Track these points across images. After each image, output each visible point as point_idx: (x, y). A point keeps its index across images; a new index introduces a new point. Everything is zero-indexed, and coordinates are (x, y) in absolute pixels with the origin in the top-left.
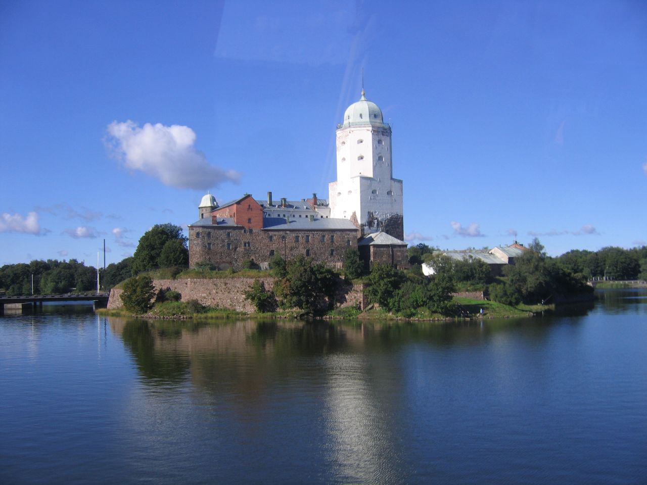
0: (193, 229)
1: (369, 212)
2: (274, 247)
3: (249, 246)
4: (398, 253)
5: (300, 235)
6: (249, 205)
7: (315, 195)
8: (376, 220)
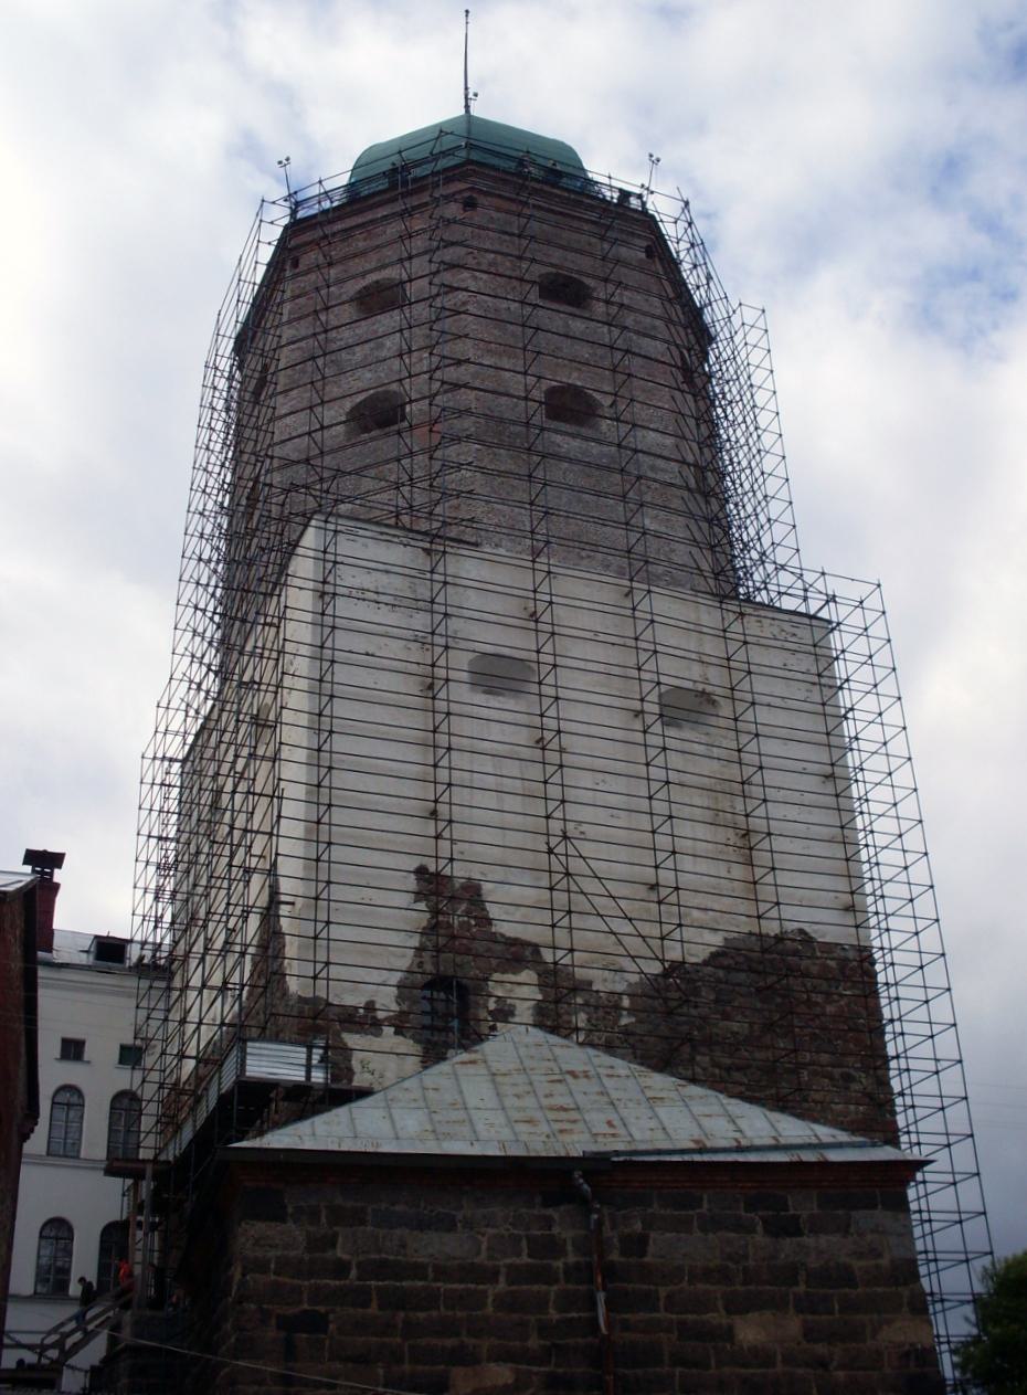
4: (750, 1332)
8: (528, 976)
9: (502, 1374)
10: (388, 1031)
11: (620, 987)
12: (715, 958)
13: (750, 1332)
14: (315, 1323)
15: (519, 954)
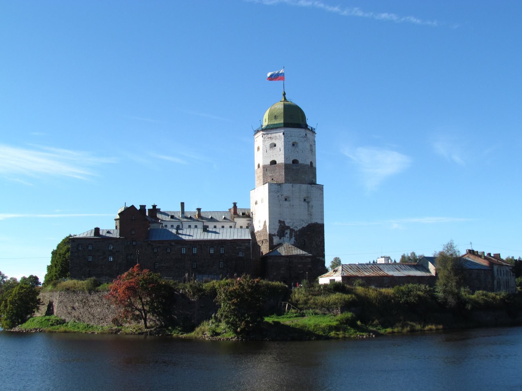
4: (299, 266)
7: (235, 204)
8: (289, 230)
9: (284, 268)
10: (276, 236)
11: (297, 230)
12: (307, 226)
13: (299, 266)
15: (288, 227)
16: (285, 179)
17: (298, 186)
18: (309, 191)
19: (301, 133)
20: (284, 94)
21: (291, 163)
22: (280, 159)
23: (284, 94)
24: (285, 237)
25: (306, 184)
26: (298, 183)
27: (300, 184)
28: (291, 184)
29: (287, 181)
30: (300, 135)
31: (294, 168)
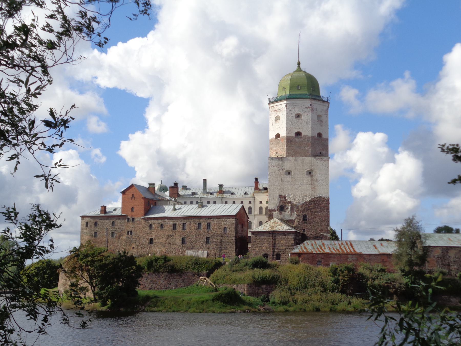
0: (83, 219)
1: (280, 195)
2: (153, 235)
3: (131, 234)
4: (282, 242)
5: (177, 223)
6: (133, 194)
8: (290, 204)
9: (266, 244)
13: (282, 242)
14: (256, 241)
15: (290, 202)
16: (287, 152)
17: (300, 159)
18: (313, 164)
19: (306, 104)
20: (299, 64)
21: (294, 135)
22: (283, 134)
23: (299, 64)
24: (286, 212)
25: (309, 156)
26: (301, 156)
27: (303, 157)
28: (294, 158)
29: (288, 154)
30: (304, 106)
31: (297, 140)
